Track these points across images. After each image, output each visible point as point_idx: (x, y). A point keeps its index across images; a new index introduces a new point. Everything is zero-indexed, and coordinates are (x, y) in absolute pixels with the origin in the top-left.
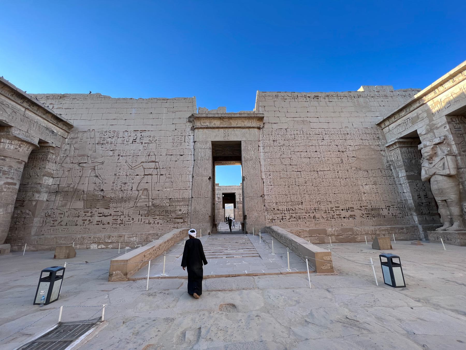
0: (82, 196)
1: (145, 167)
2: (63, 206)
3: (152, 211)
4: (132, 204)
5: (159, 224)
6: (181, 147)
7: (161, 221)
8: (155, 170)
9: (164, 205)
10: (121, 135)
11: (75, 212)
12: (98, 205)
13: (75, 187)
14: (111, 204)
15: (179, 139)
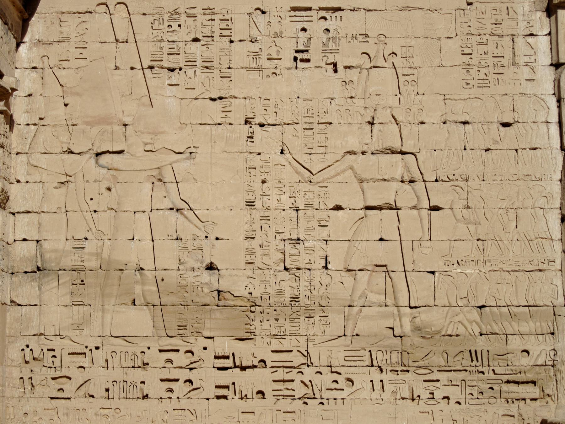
0: (139, 289)
1: (365, 176)
2: (78, 326)
3: (419, 354)
4: (336, 323)
5: (452, 402)
6: (501, 89)
7: (455, 393)
8: (406, 186)
9: (461, 330)
10: (240, 29)
11: (131, 349)
12: (208, 324)
13: (105, 255)
14: (257, 323)
15: (490, 48)
